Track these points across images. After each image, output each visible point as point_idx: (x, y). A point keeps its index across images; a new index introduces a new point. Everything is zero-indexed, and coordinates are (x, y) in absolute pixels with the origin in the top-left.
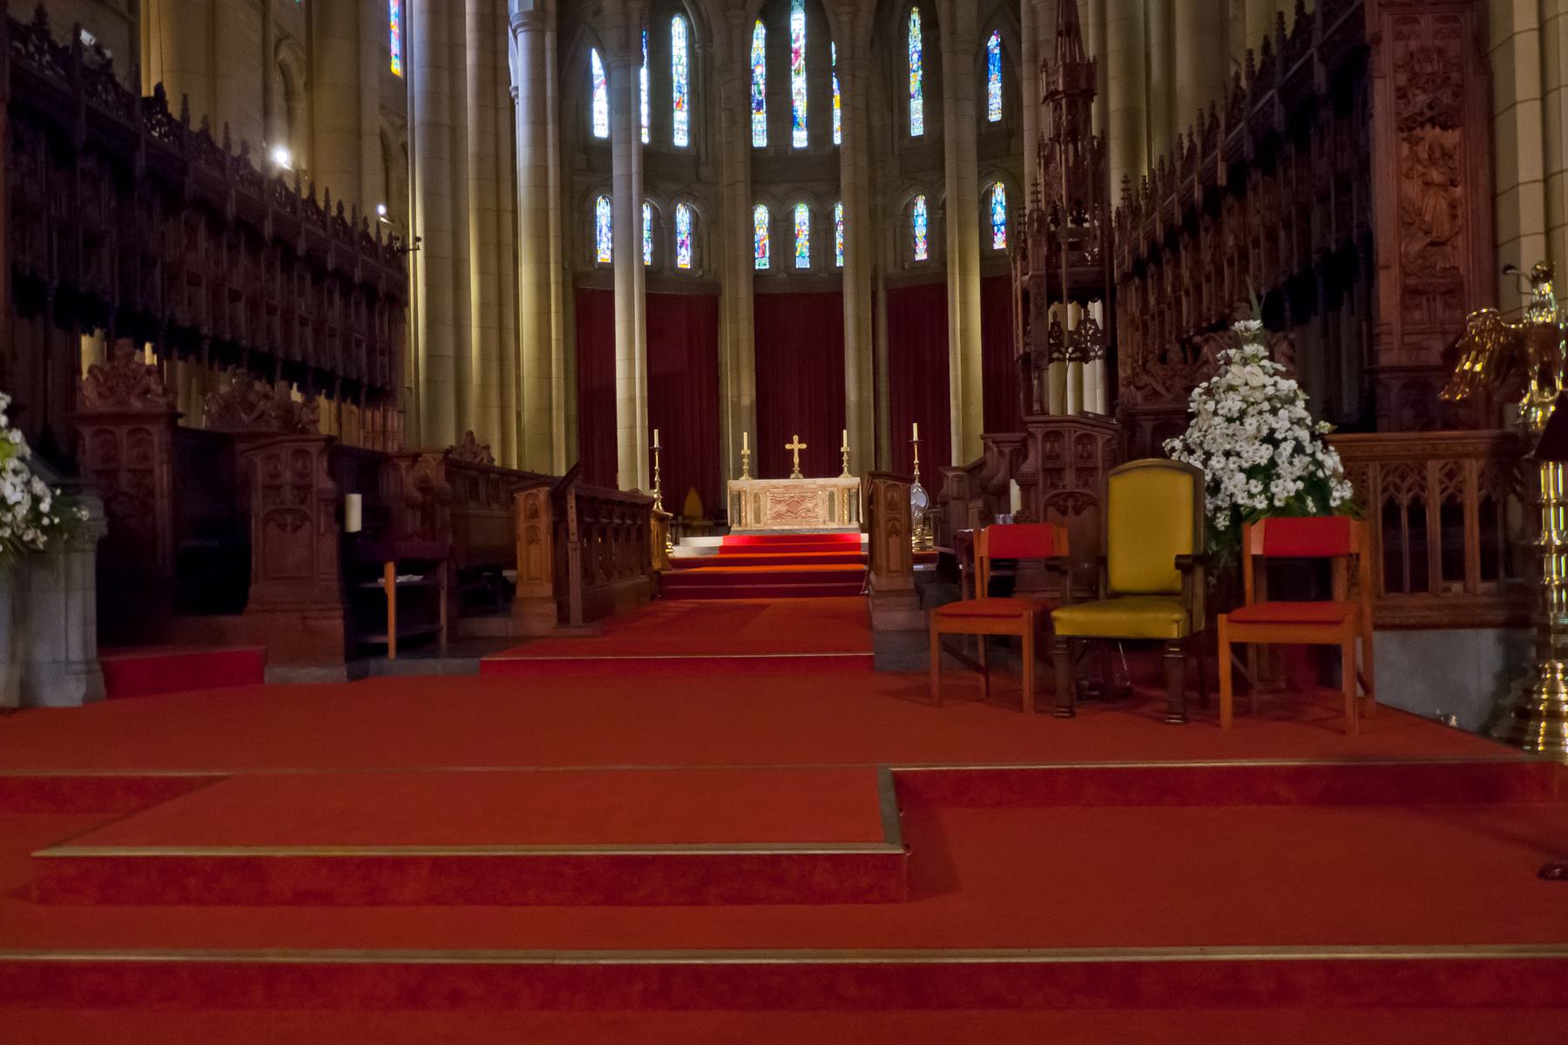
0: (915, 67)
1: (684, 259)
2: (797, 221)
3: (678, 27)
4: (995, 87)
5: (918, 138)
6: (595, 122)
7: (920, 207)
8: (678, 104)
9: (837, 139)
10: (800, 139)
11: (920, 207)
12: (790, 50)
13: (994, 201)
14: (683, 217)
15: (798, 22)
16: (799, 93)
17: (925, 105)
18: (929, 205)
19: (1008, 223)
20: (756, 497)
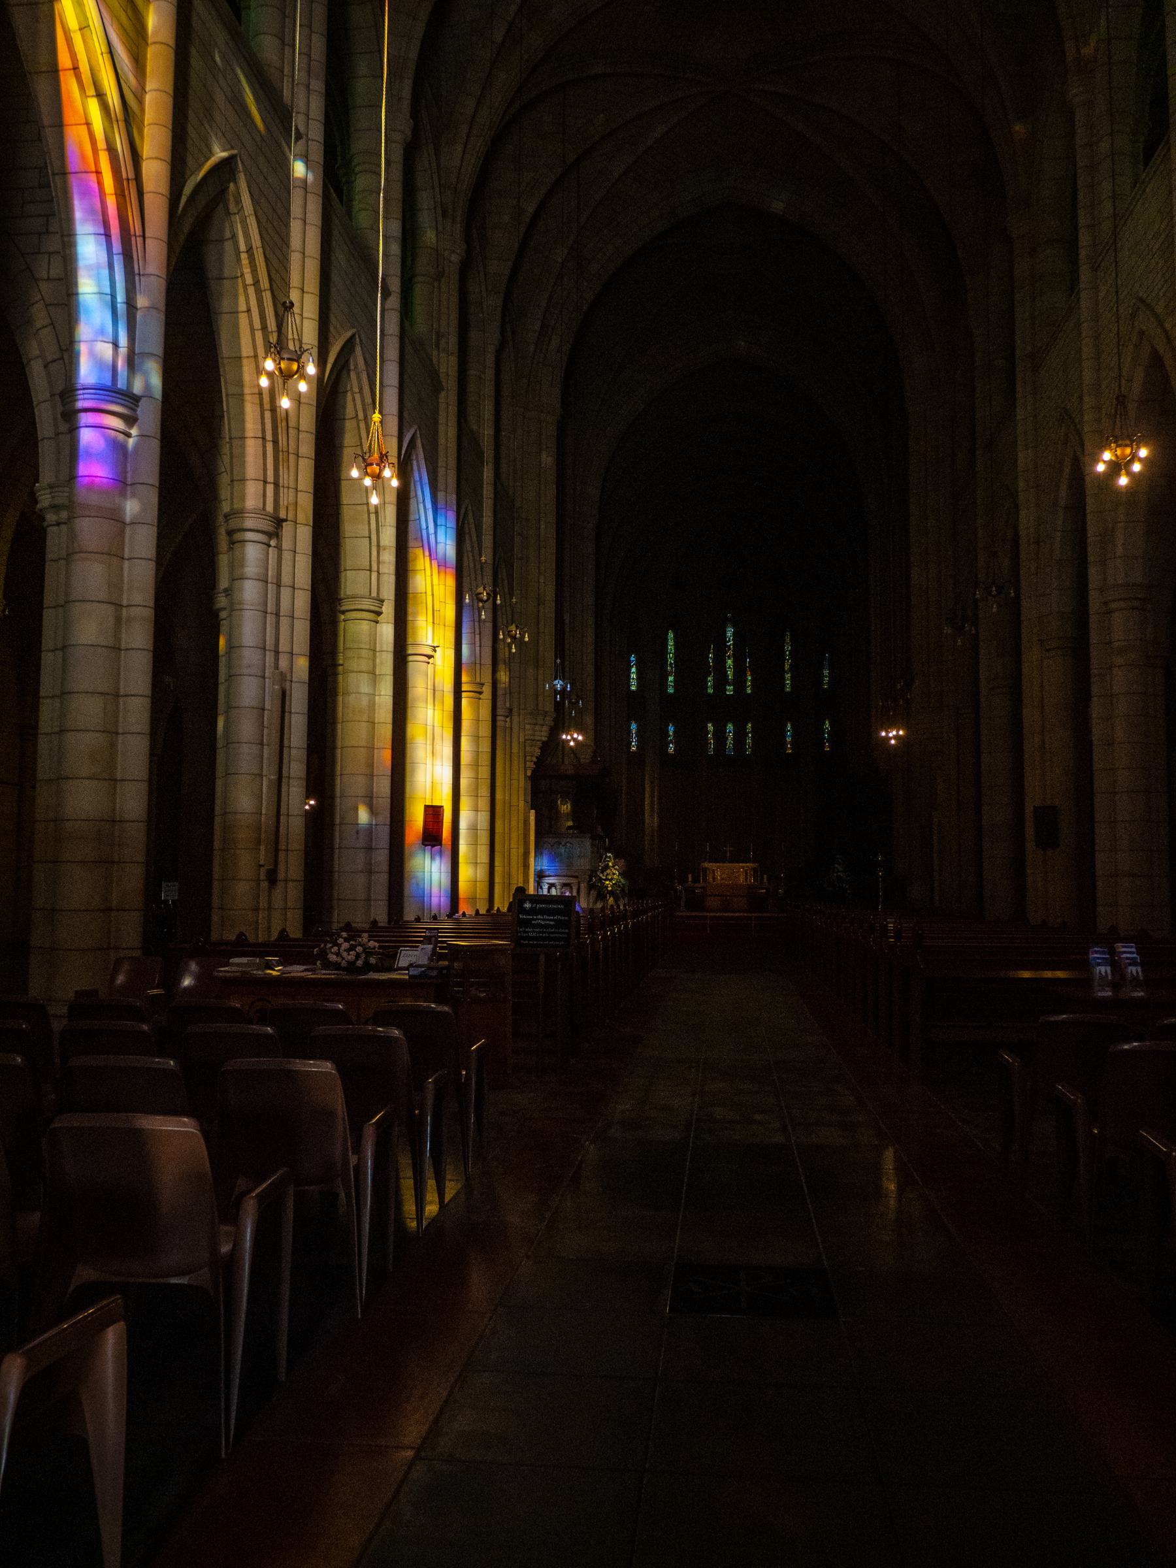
3: (671, 635)
4: (826, 672)
9: (749, 691)
10: (730, 690)
14: (671, 729)
15: (730, 632)
16: (729, 668)
17: (791, 677)
20: (714, 871)
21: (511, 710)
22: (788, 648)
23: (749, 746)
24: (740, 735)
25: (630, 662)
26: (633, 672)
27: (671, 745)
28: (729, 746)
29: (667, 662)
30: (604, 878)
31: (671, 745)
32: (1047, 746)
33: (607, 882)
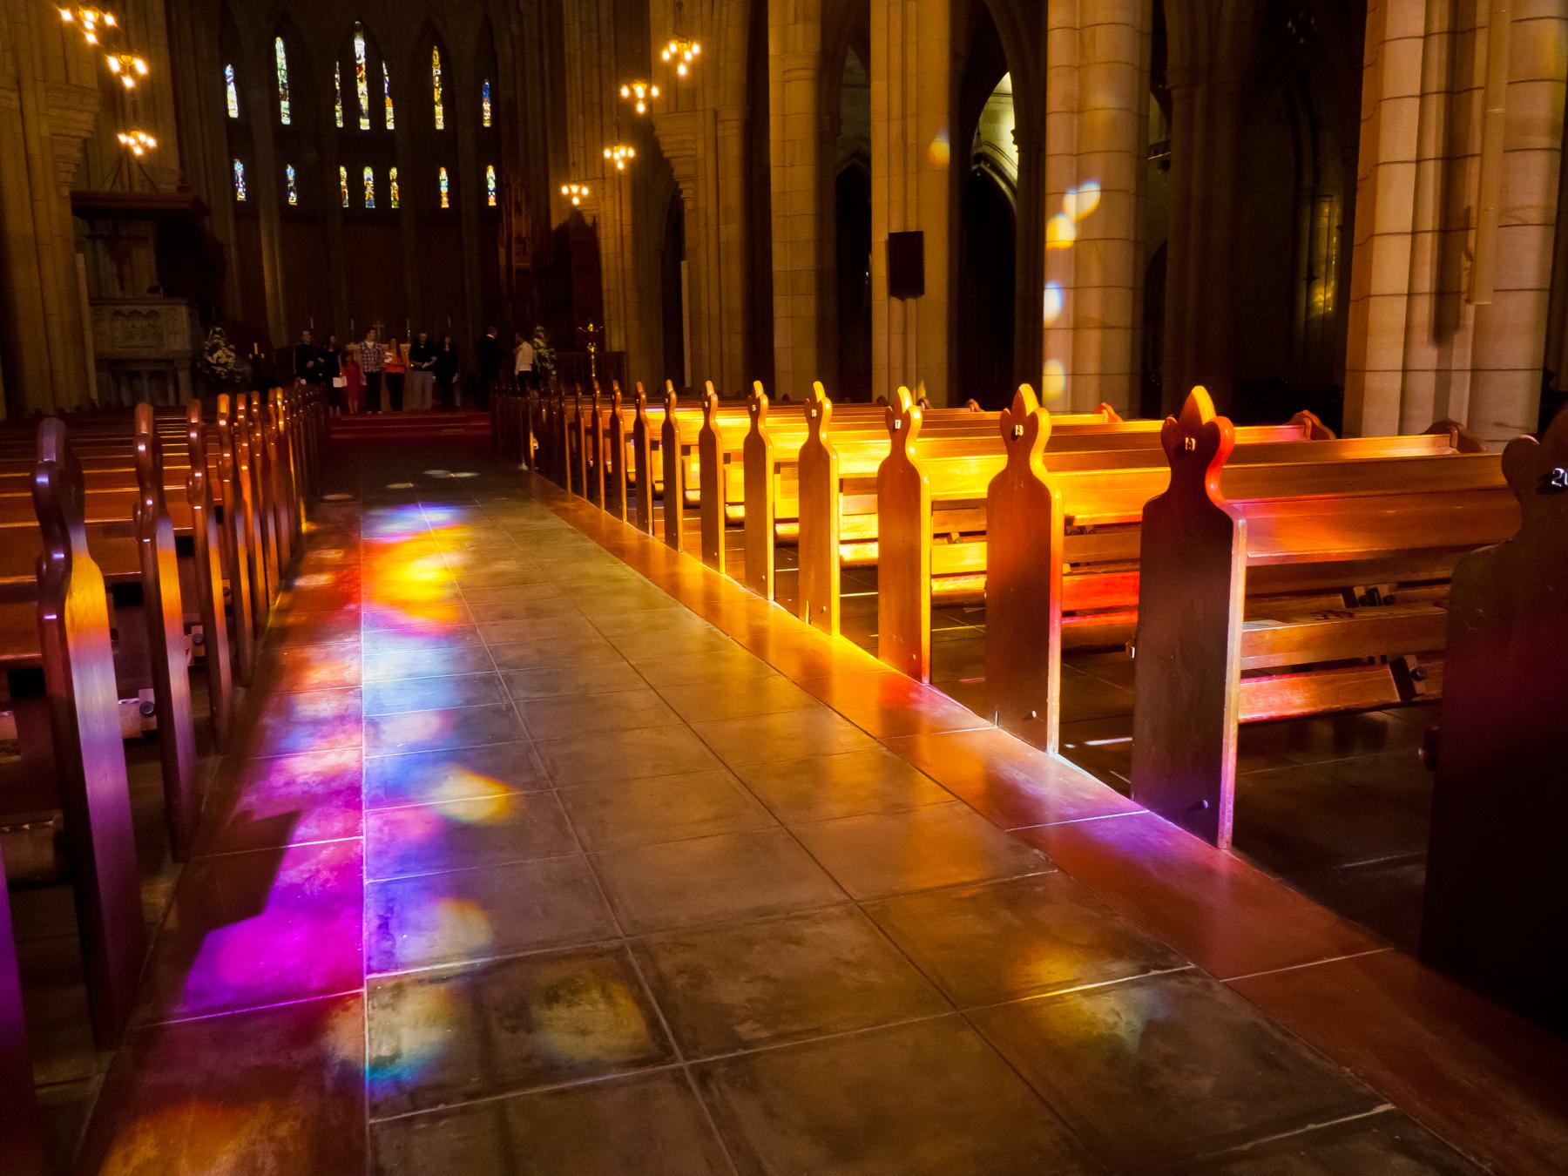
0: (437, 85)
1: (293, 199)
2: (365, 178)
3: (279, 44)
4: (487, 106)
5: (440, 131)
6: (229, 108)
7: (443, 174)
8: (283, 96)
9: (390, 126)
10: (365, 124)
11: (443, 174)
12: (356, 65)
13: (488, 176)
14: (291, 172)
15: (360, 46)
16: (363, 94)
18: (448, 174)
19: (497, 190)
21: (18, 82)
22: (437, 71)
23: (395, 199)
24: (382, 183)
25: (224, 77)
26: (232, 92)
27: (292, 194)
28: (369, 198)
29: (278, 81)
30: (214, 362)
31: (292, 194)
32: (911, 140)
33: (220, 369)
